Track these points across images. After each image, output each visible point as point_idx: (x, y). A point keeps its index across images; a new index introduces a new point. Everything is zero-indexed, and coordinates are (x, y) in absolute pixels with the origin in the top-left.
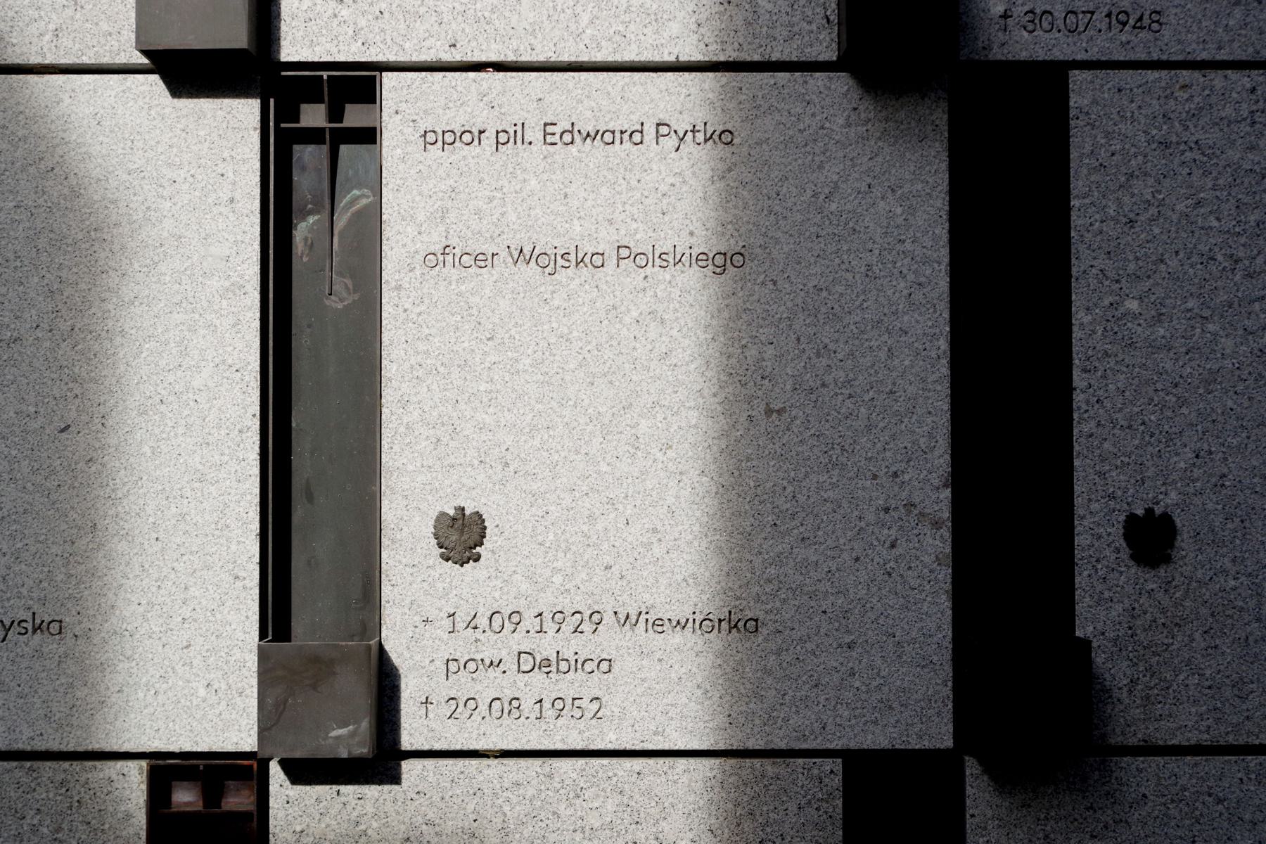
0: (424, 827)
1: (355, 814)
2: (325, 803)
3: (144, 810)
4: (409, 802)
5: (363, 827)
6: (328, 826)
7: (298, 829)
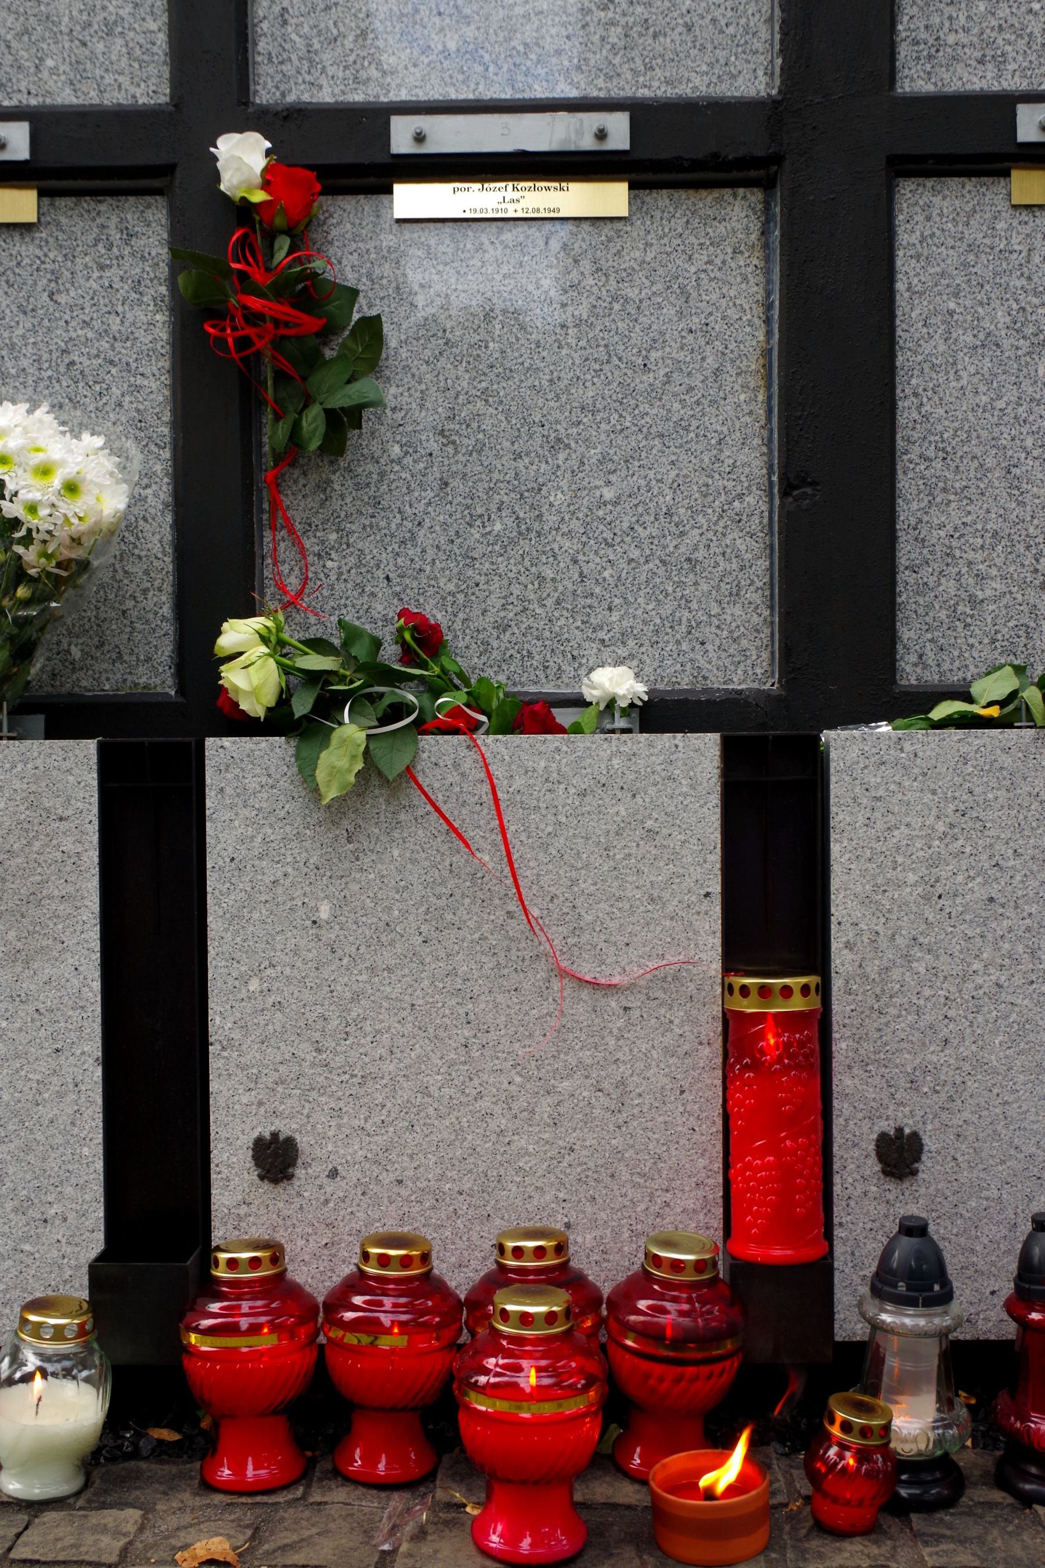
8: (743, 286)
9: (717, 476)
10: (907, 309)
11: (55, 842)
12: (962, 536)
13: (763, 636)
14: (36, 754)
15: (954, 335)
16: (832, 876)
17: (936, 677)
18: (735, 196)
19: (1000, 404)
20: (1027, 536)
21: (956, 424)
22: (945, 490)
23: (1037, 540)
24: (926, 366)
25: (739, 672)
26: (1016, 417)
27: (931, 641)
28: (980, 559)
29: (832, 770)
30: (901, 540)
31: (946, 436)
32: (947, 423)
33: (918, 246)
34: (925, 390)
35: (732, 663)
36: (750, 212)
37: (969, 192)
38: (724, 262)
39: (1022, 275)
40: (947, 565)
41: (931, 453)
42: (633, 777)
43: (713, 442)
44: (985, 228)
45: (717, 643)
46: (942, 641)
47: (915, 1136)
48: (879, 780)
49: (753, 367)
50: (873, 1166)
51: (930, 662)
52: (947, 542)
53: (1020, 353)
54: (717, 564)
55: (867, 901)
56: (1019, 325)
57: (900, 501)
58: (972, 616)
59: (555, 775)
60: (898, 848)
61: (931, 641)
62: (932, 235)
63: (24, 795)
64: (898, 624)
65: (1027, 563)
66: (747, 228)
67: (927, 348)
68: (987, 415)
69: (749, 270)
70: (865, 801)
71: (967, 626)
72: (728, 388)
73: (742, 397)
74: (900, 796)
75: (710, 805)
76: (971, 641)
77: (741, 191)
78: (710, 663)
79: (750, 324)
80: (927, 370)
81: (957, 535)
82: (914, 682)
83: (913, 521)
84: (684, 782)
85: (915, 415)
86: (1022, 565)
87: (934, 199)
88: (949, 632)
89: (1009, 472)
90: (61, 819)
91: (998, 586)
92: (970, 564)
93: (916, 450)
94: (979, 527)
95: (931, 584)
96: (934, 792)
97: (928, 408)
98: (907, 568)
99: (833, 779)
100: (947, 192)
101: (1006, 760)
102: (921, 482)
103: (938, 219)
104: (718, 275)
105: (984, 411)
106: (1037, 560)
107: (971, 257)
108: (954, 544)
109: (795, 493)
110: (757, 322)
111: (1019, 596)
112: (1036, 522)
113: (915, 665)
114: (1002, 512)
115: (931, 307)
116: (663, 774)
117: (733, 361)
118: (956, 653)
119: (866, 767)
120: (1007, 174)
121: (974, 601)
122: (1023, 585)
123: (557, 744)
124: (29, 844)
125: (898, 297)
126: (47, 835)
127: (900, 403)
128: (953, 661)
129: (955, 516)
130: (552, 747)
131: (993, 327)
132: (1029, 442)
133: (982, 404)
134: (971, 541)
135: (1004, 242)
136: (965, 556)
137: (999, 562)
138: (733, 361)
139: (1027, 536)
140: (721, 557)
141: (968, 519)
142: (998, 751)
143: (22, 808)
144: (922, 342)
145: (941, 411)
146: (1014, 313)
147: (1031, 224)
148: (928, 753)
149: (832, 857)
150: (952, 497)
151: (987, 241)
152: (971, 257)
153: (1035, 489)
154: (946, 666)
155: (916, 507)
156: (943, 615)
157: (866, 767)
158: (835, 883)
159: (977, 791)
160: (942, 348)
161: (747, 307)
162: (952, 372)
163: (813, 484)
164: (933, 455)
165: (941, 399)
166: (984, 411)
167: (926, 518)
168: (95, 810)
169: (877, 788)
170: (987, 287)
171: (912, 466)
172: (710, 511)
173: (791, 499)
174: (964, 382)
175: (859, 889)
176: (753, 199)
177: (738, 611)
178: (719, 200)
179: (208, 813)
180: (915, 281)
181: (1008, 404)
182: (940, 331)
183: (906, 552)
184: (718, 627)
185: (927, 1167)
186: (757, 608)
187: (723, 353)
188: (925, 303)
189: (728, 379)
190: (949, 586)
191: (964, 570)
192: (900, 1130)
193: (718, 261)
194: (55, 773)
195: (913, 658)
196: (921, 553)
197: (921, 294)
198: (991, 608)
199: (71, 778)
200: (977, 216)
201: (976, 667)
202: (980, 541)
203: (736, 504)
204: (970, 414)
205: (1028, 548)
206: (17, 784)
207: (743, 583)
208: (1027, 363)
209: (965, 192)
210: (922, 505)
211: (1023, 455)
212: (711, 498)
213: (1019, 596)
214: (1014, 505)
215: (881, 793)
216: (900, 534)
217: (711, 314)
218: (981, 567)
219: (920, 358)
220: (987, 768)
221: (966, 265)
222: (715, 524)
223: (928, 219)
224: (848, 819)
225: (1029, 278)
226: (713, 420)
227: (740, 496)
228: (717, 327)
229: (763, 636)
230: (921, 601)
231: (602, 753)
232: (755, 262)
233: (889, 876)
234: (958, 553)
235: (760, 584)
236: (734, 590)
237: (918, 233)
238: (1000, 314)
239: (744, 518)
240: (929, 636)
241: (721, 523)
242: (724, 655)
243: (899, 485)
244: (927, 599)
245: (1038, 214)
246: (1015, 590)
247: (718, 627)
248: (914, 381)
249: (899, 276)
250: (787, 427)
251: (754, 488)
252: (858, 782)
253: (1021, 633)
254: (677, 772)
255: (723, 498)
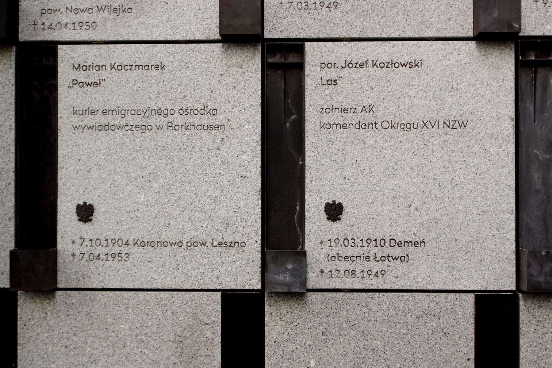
11: (203, 333)
14: (196, 298)
16: (520, 352)
29: (520, 310)
42: (439, 311)
55: (535, 363)
59: (407, 310)
60: (548, 342)
63: (191, 314)
70: (534, 322)
74: (548, 320)
75: (470, 323)
84: (459, 313)
90: (206, 324)
99: (521, 313)
116: (451, 310)
119: (534, 308)
123: (408, 297)
124: (193, 334)
126: (200, 331)
130: (406, 298)
143: (190, 319)
149: (520, 345)
158: (521, 356)
168: (220, 321)
169: (539, 317)
175: (531, 358)
179: (265, 323)
194: (204, 306)
199: (210, 308)
206: (188, 310)
215: (541, 319)
224: (527, 330)
231: (426, 301)
233: (544, 353)
254: (457, 309)
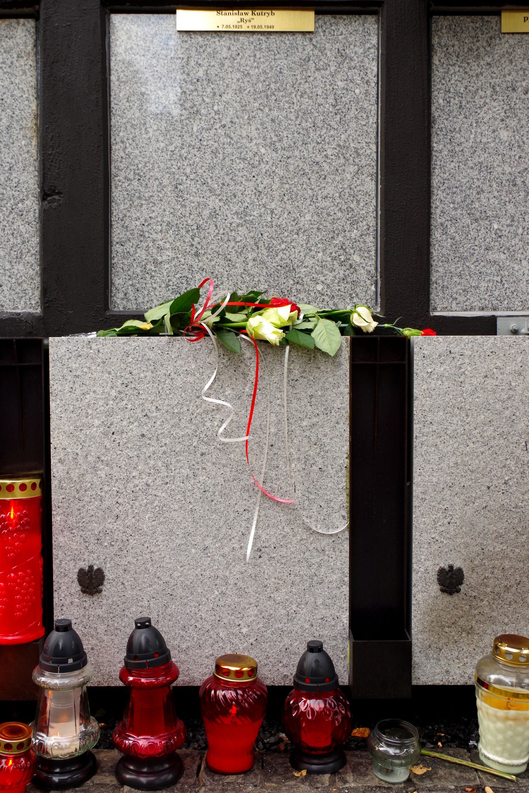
0: (495, 370)
1: (459, 363)
2: (443, 357)
3: (348, 361)
4: (487, 357)
5: (462, 370)
6: (445, 369)
7: (429, 371)
8: (24, 77)
9: (8, 189)
10: (117, 92)
12: (149, 224)
13: (35, 282)
15: (145, 107)
16: (51, 421)
17: (135, 306)
18: (18, 23)
19: (171, 148)
20: (187, 225)
21: (146, 160)
22: (139, 198)
23: (193, 227)
24: (128, 125)
25: (22, 303)
26: (180, 156)
27: (132, 285)
28: (160, 238)
29: (50, 360)
30: (114, 227)
31: (140, 166)
32: (140, 159)
33: (124, 54)
34: (128, 139)
35: (18, 297)
36: (27, 34)
37: (153, 23)
38: (12, 63)
39: (184, 72)
40: (141, 241)
41: (131, 176)
43: (6, 168)
44: (162, 44)
45: (9, 285)
46: (138, 285)
47: (100, 570)
48: (77, 366)
49: (29, 125)
50: (76, 587)
51: (131, 297)
52: (140, 228)
53: (183, 118)
54: (9, 240)
55: (71, 435)
56: (182, 101)
57: (113, 204)
58: (155, 271)
60: (89, 405)
61: (132, 285)
62: (131, 48)
64: (113, 275)
65: (187, 240)
66: (25, 43)
67: (129, 114)
68: (164, 154)
69: (27, 67)
70: (69, 378)
71: (152, 277)
72: (15, 137)
73: (23, 142)
74: (90, 375)
76: (155, 285)
77: (22, 21)
78: (5, 297)
79: (28, 99)
80: (129, 127)
81: (146, 224)
82: (121, 309)
83: (121, 216)
85: (122, 154)
86: (184, 242)
87: (132, 27)
88: (142, 280)
89: (177, 188)
91: (170, 254)
92: (154, 241)
93: (122, 174)
94: (159, 219)
95: (132, 253)
96: (109, 373)
97: (129, 150)
98: (117, 243)
100: (140, 23)
101: (151, 355)
102: (126, 193)
103: (135, 38)
104: (9, 70)
105: (162, 152)
106: (193, 239)
107: (154, 61)
108: (145, 229)
109: (49, 198)
110: (32, 98)
111: (182, 260)
112: (192, 217)
113: (123, 299)
114: (172, 211)
115: (131, 90)
117: (17, 121)
118: (146, 293)
119: (70, 358)
120: (174, 13)
121: (156, 263)
122: (185, 253)
125: (112, 84)
127: (113, 147)
128: (144, 297)
129: (145, 213)
131: (167, 103)
132: (188, 170)
133: (161, 148)
134: (155, 227)
135: (173, 52)
136: (151, 236)
137: (170, 240)
138: (17, 121)
139: (187, 225)
140: (11, 236)
141: (153, 215)
142: (147, 349)
144: (126, 111)
145: (137, 152)
146: (179, 94)
147: (189, 42)
148: (106, 350)
149: (51, 410)
150: (143, 202)
151: (164, 52)
152: (154, 61)
153: (191, 198)
154: (140, 300)
155: (123, 208)
156: (138, 270)
157: (70, 358)
159: (134, 372)
160: (137, 114)
161: (25, 89)
162: (143, 129)
163: (59, 193)
164: (132, 177)
165: (137, 145)
166: (162, 152)
167: (128, 214)
169: (76, 370)
170: (164, 79)
171: (120, 184)
172: (4, 209)
173: (46, 202)
174: (150, 135)
175: (66, 428)
176: (29, 25)
177: (21, 267)
178: (9, 26)
180: (122, 75)
181: (176, 148)
182: (136, 105)
183: (117, 233)
184: (10, 276)
185: (107, 588)
186: (32, 265)
187: (12, 117)
188: (128, 88)
189: (15, 132)
190: (142, 254)
191: (151, 244)
192: (91, 567)
193: (9, 62)
195: (121, 295)
196: (126, 235)
197: (125, 83)
198: (166, 266)
200: (158, 37)
201: (158, 300)
202: (159, 228)
203: (20, 205)
204: (154, 154)
205: (188, 232)
207: (24, 251)
208: (187, 124)
209: (150, 23)
210: (126, 207)
211: (185, 178)
212: (5, 202)
213: (182, 260)
214: (179, 207)
215: (78, 373)
216: (113, 223)
217: (4, 93)
218: (160, 242)
219: (125, 120)
220: (140, 359)
221: (151, 66)
222: (8, 217)
223: (129, 38)
224: (60, 388)
225: (188, 74)
226: (6, 156)
227: (22, 201)
228: (8, 101)
229: (35, 282)
230: (126, 262)
232: (31, 63)
233: (83, 421)
234: (147, 235)
235: (33, 252)
236: (19, 255)
237: (123, 47)
238: (171, 95)
239: (25, 213)
240: (130, 282)
241: (11, 216)
242: (13, 293)
243: (113, 195)
244: (129, 261)
245: (193, 36)
246: (180, 256)
247: (10, 276)
248: (121, 134)
249: (112, 72)
250: (43, 160)
251: (30, 196)
252: (65, 367)
253: (183, 281)
255: (12, 201)
